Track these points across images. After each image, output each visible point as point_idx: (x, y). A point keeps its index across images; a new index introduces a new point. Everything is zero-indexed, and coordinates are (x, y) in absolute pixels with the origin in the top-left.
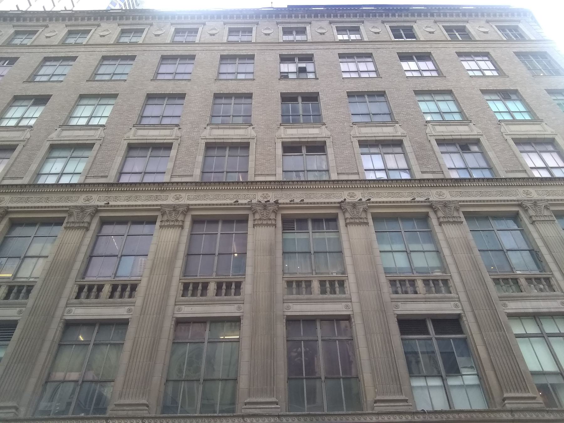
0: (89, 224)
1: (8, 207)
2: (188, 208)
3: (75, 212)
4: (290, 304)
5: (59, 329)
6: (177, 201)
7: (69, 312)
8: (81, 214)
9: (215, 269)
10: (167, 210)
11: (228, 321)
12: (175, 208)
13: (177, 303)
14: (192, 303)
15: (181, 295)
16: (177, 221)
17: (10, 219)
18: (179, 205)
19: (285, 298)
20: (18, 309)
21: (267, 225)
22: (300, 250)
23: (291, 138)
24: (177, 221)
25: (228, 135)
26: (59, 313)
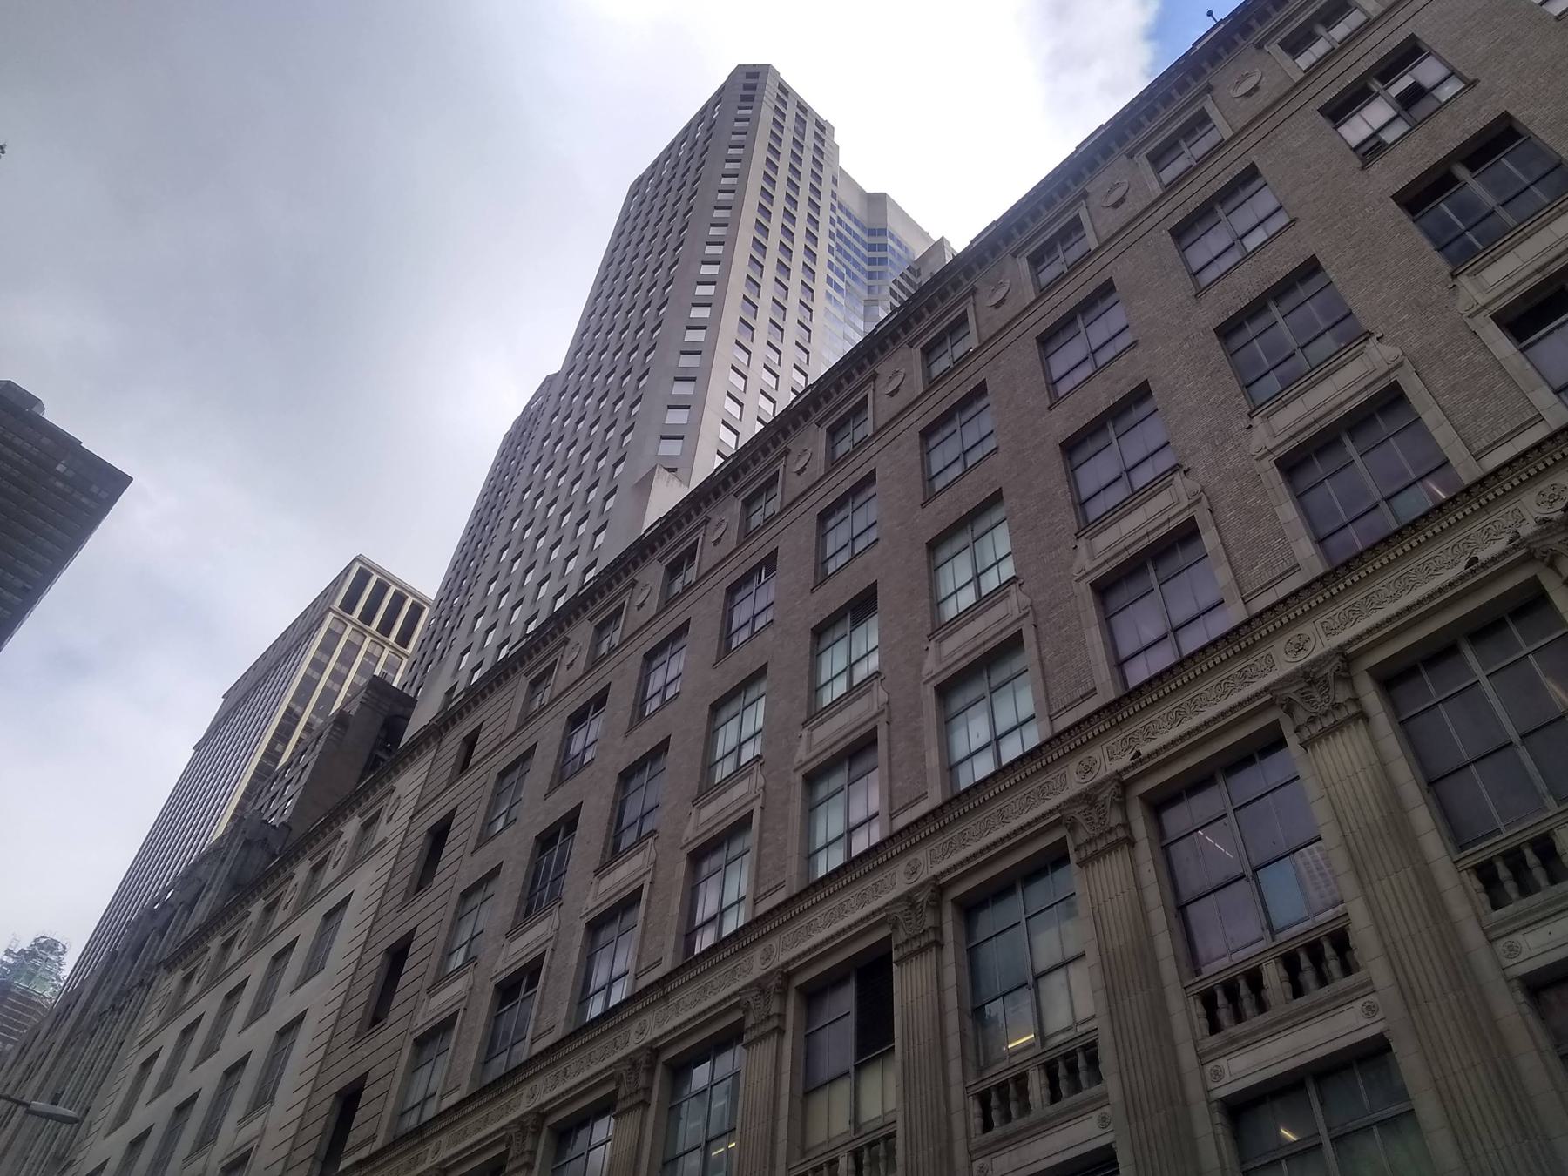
0: (1127, 826)
1: (935, 877)
3: (1077, 812)
6: (1302, 655)
8: (1094, 811)
10: (1291, 692)
12: (1308, 677)
16: (1337, 707)
18: (1313, 663)
20: (1095, 1115)
23: (1511, 289)
24: (1337, 707)
25: (1324, 403)
26: (1194, 1090)
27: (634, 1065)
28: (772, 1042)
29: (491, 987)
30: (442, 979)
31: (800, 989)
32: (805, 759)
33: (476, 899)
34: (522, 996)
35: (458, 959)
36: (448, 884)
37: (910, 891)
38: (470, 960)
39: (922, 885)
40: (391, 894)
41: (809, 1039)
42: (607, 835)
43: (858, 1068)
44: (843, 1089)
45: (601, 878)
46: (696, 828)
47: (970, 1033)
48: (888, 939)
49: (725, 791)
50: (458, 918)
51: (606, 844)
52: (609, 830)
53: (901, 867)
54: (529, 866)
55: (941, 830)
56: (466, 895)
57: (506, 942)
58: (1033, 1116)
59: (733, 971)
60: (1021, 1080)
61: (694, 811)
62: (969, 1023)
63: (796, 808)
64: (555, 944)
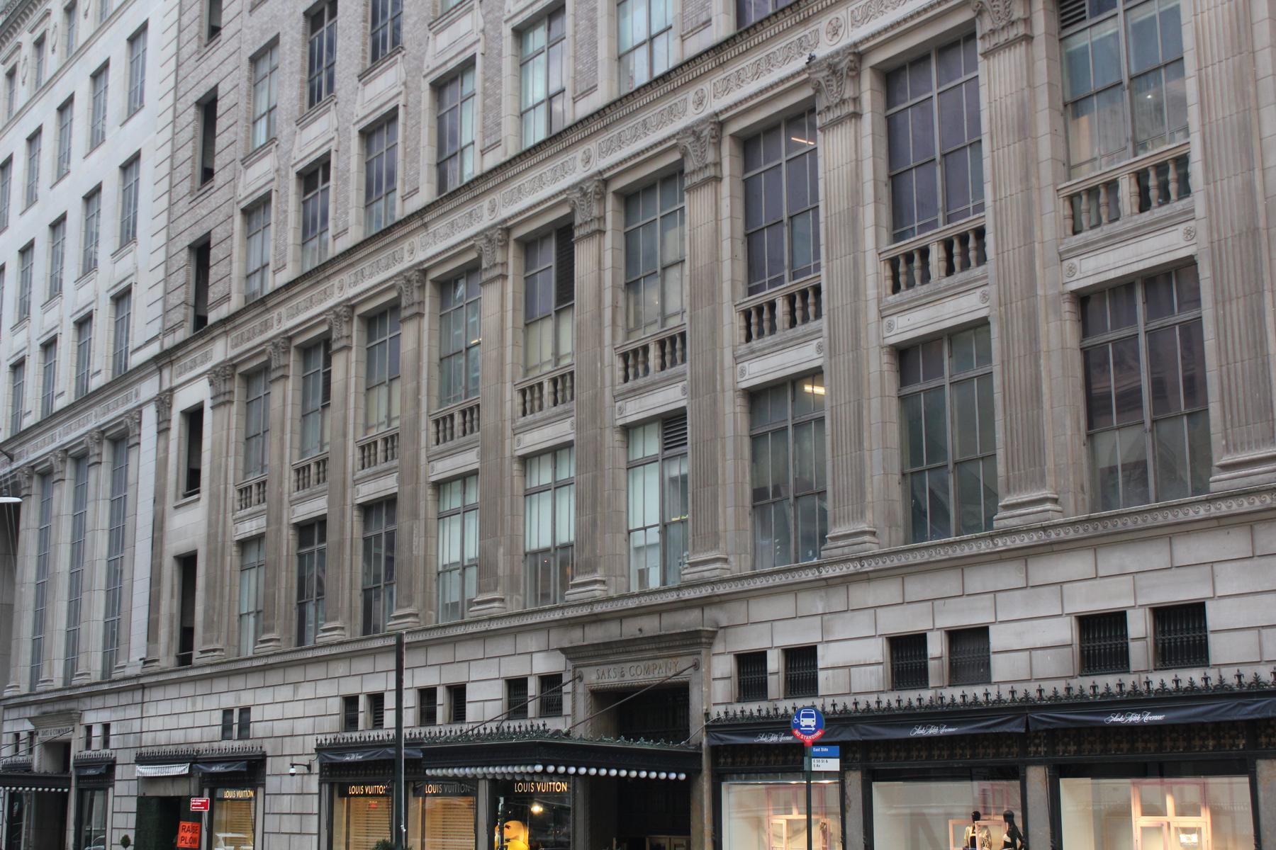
0: (718, 164)
1: (600, 173)
2: (857, 55)
4: (1075, 261)
5: (738, 409)
6: (836, 39)
7: (743, 372)
9: (940, 204)
10: (821, 76)
11: (971, 329)
13: (885, 313)
14: (906, 307)
15: (889, 291)
16: (843, 101)
17: (615, 193)
18: (837, 53)
19: (1062, 248)
21: (1009, 44)
22: (1100, 87)
26: (728, 381)
27: (409, 281)
28: (498, 284)
29: (292, 175)
30: (248, 159)
31: (518, 240)
32: (514, 10)
33: (264, 67)
34: (320, 187)
35: (261, 139)
36: (234, 44)
37: (584, 181)
38: (271, 140)
39: (591, 177)
40: (185, 36)
41: (529, 281)
42: (364, 34)
43: (558, 312)
44: (548, 326)
45: (365, 84)
46: (435, 57)
47: (622, 303)
48: (571, 216)
49: (453, 22)
50: (255, 84)
51: (364, 44)
52: (365, 28)
53: (579, 153)
54: (304, 45)
55: (606, 127)
56: (255, 60)
57: (298, 129)
58: (649, 378)
59: (471, 214)
60: (646, 349)
61: (430, 35)
62: (621, 296)
63: (508, 64)
64: (339, 142)
